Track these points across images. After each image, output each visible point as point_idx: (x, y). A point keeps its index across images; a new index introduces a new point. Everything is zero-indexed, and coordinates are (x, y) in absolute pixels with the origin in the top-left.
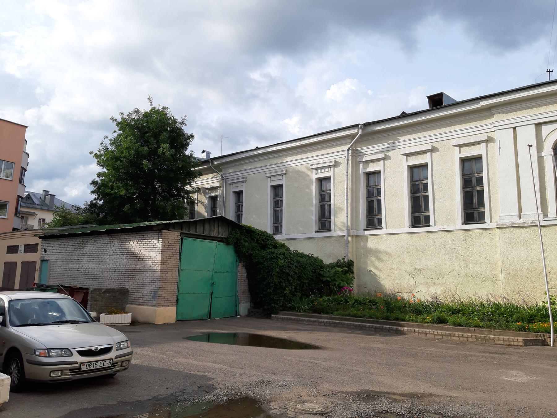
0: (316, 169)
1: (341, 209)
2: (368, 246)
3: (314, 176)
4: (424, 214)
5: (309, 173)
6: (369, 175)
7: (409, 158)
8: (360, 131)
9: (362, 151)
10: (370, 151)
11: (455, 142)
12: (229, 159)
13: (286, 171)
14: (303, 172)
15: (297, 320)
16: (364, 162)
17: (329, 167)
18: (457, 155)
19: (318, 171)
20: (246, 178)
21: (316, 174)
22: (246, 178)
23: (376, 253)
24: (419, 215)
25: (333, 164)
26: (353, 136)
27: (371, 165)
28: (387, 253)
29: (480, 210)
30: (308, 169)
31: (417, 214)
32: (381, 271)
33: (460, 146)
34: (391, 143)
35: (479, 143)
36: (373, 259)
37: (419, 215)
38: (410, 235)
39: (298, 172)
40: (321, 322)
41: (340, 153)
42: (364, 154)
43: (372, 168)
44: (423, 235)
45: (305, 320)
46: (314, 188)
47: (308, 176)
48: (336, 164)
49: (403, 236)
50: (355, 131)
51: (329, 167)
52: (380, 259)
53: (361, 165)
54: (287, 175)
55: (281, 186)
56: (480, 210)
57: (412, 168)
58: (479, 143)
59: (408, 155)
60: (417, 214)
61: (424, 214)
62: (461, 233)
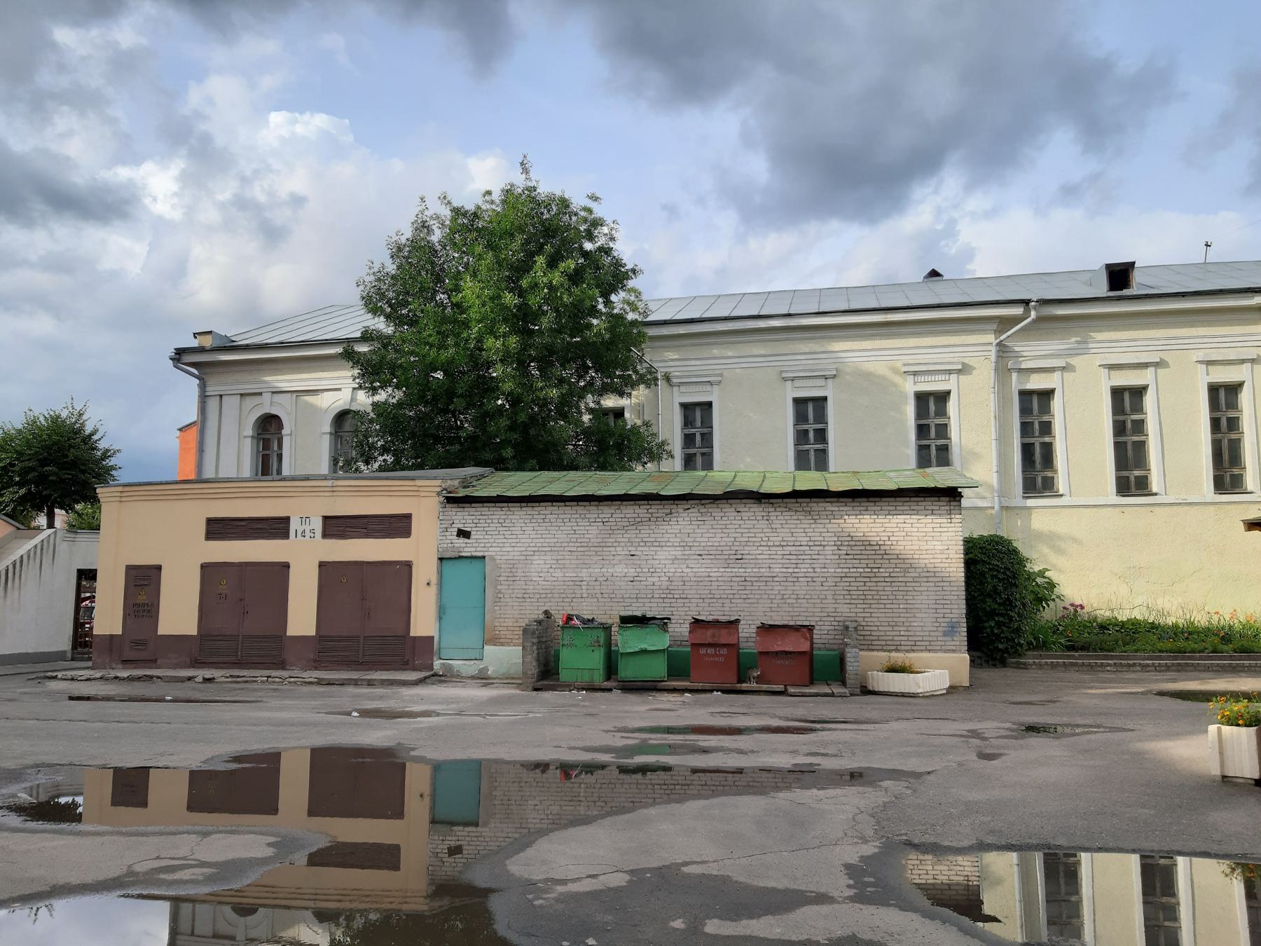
0: (915, 373)
1: (977, 456)
2: (1033, 526)
3: (911, 387)
4: (1137, 473)
5: (898, 379)
6: (1025, 395)
7: (1112, 372)
8: (1033, 314)
9: (1016, 349)
10: (1033, 351)
11: (1201, 355)
12: (682, 330)
13: (837, 370)
14: (883, 378)
15: (1090, 665)
16: (1020, 370)
17: (950, 372)
18: (1202, 380)
19: (920, 378)
20: (721, 375)
21: (915, 383)
22: (721, 375)
23: (1051, 539)
24: (1131, 475)
25: (960, 367)
26: (1015, 320)
27: (1034, 377)
28: (1075, 540)
29: (1236, 471)
30: (895, 371)
31: (1125, 473)
32: (1060, 571)
33: (1209, 363)
34: (1078, 342)
35: (1243, 361)
36: (1045, 550)
37: (1131, 475)
38: (1118, 510)
39: (868, 376)
40: (1148, 665)
41: (978, 349)
42: (1018, 356)
43: (1037, 383)
44: (1143, 509)
45: (1109, 665)
46: (910, 410)
47: (896, 385)
48: (964, 370)
49: (1105, 510)
50: (1018, 311)
51: (950, 372)
52: (1060, 551)
53: (1014, 375)
54: (837, 380)
55: (825, 399)
56: (1236, 471)
57: (1117, 393)
58: (1243, 361)
59: (1112, 367)
60: (1125, 473)
61: (1137, 473)
62: (1212, 508)
